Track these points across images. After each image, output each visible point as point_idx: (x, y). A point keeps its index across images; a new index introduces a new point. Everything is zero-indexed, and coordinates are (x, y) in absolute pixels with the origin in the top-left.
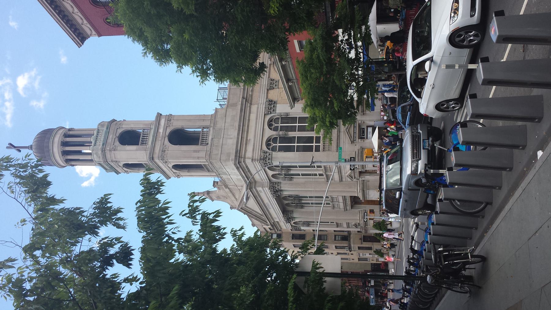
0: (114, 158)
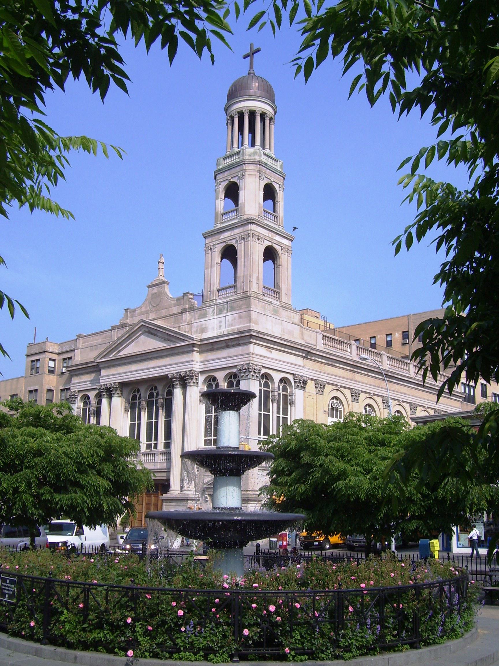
0: (249, 173)
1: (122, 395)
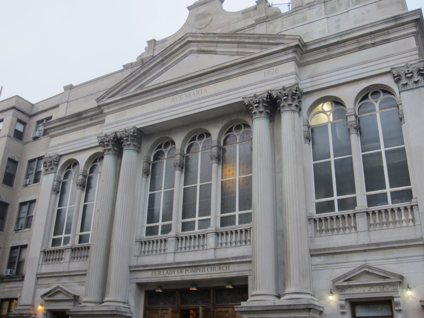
1: (138, 150)
